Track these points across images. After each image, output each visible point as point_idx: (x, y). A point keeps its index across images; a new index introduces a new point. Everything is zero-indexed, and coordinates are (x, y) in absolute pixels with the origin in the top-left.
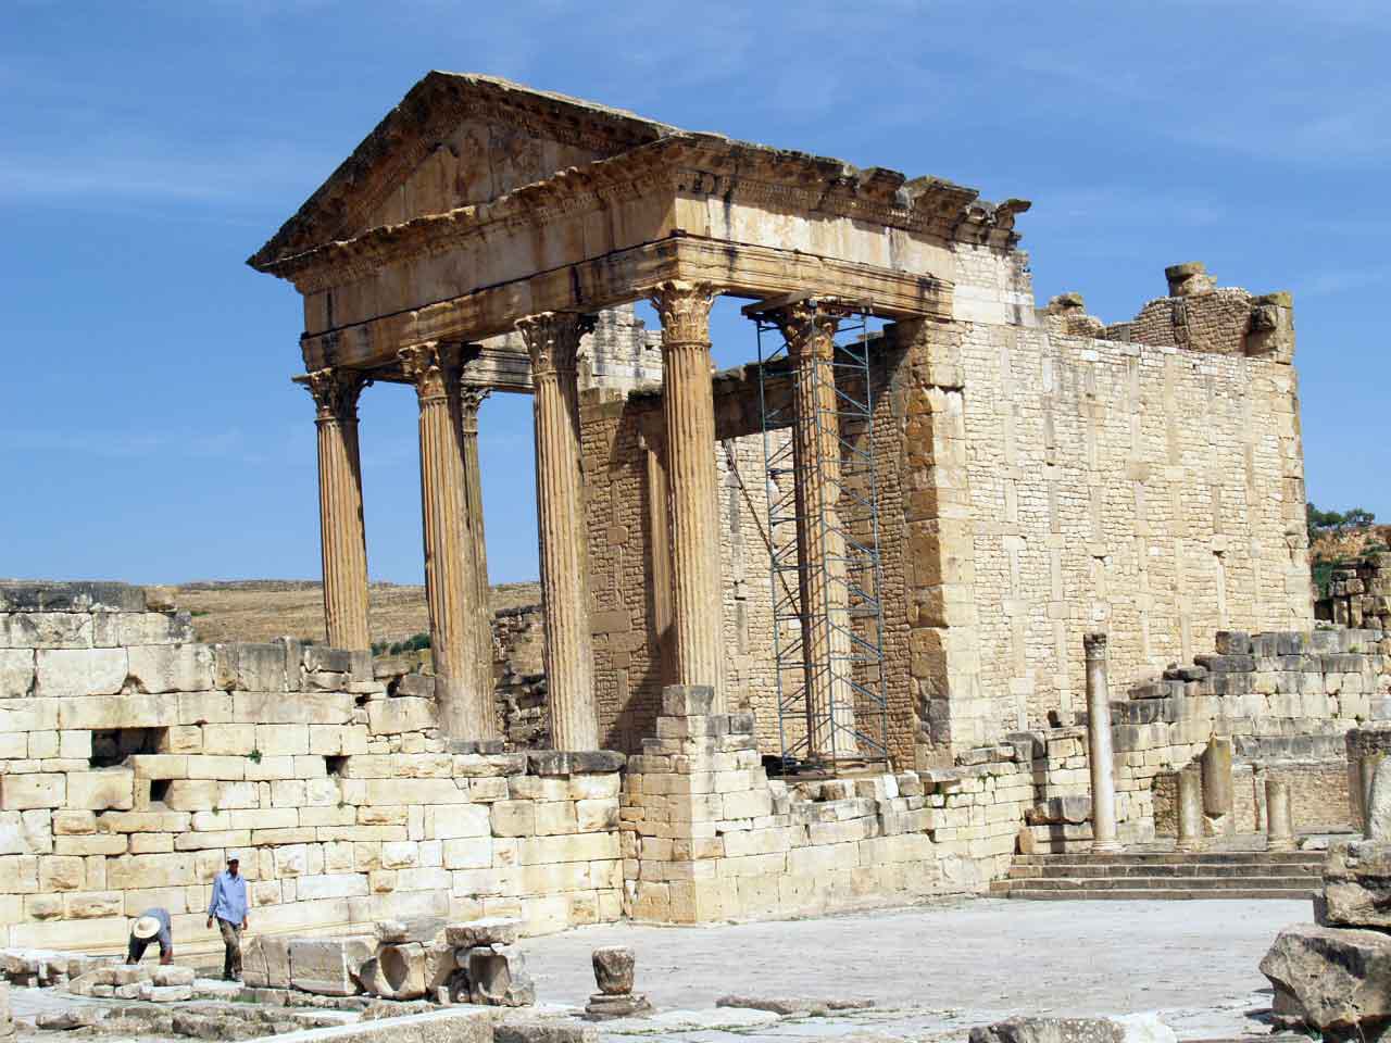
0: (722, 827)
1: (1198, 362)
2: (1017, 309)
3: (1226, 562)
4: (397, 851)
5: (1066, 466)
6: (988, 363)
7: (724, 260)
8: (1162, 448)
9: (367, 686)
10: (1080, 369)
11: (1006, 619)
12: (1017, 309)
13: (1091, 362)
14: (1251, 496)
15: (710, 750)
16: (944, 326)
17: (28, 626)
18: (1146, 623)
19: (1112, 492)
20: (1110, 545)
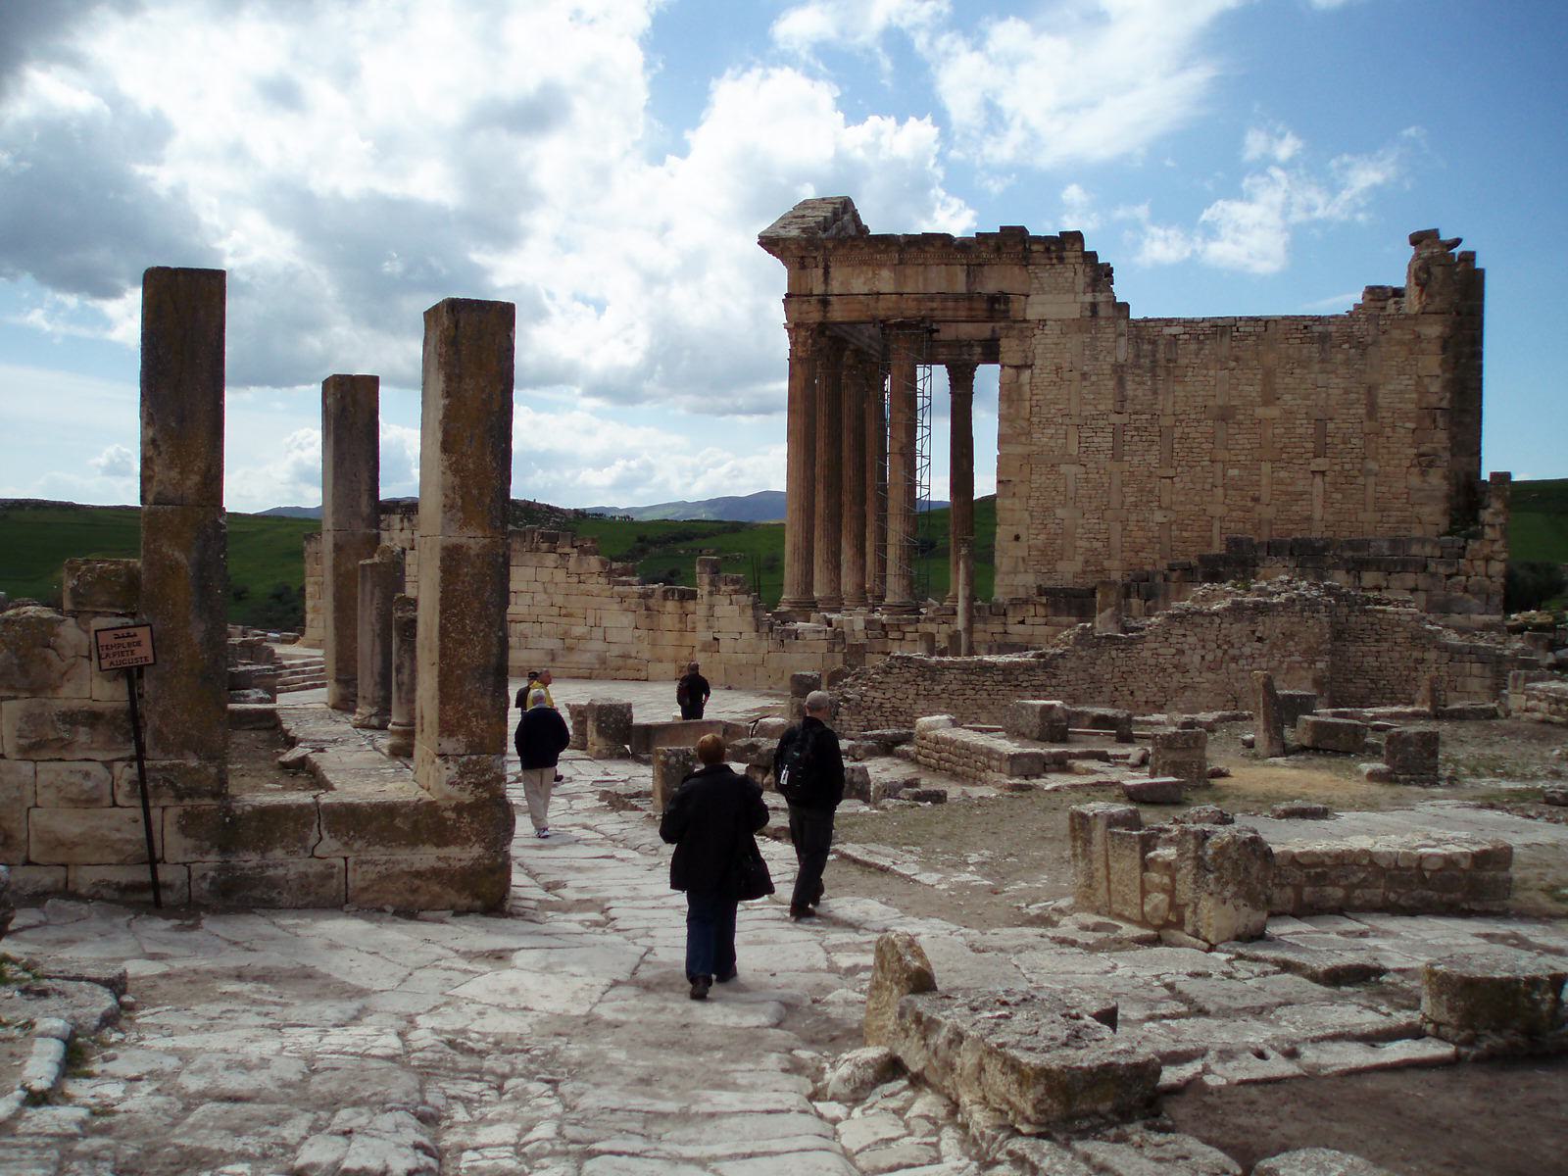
0: (717, 636)
1: (1311, 323)
2: (1094, 306)
3: (1327, 479)
4: (579, 630)
5: (1136, 413)
6: (1062, 346)
7: (819, 307)
8: (1254, 394)
9: (567, 550)
10: (1161, 342)
11: (1057, 521)
12: (1094, 306)
13: (1175, 336)
14: (1368, 426)
15: (711, 593)
16: (1017, 325)
17: (409, 520)
18: (1217, 524)
19: (1186, 430)
20: (1179, 469)
